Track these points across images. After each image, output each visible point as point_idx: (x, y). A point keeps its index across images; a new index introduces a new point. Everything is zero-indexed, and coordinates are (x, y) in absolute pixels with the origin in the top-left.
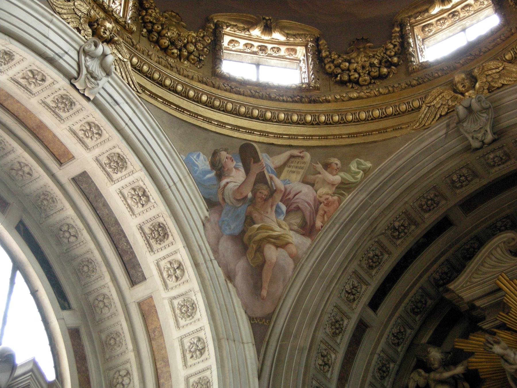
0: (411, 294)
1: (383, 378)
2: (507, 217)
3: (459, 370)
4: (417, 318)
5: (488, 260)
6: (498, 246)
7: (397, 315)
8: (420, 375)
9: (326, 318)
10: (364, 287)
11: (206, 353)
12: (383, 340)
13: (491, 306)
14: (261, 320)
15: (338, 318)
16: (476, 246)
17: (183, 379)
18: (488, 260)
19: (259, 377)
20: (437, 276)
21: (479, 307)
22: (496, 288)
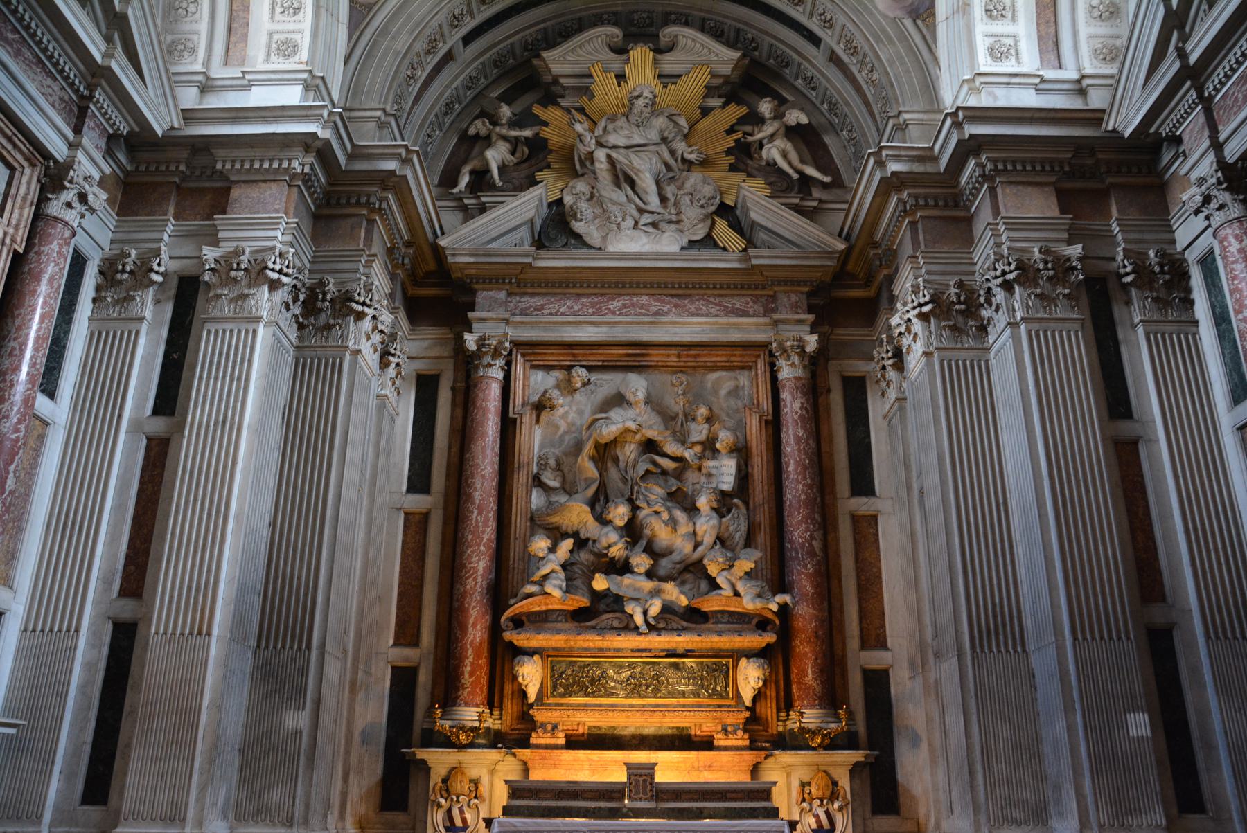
0: (502, 46)
1: (446, 114)
2: (615, 14)
3: (528, 133)
4: (495, 71)
5: (587, 44)
6: (600, 36)
7: (481, 60)
8: (484, 124)
9: (428, 32)
10: (469, 18)
11: (301, 15)
12: (461, 78)
13: (573, 88)
14: (360, 6)
15: (437, 37)
16: (575, 27)
17: (266, 33)
18: (587, 44)
19: (346, 63)
20: (530, 40)
21: (561, 85)
22: (587, 73)
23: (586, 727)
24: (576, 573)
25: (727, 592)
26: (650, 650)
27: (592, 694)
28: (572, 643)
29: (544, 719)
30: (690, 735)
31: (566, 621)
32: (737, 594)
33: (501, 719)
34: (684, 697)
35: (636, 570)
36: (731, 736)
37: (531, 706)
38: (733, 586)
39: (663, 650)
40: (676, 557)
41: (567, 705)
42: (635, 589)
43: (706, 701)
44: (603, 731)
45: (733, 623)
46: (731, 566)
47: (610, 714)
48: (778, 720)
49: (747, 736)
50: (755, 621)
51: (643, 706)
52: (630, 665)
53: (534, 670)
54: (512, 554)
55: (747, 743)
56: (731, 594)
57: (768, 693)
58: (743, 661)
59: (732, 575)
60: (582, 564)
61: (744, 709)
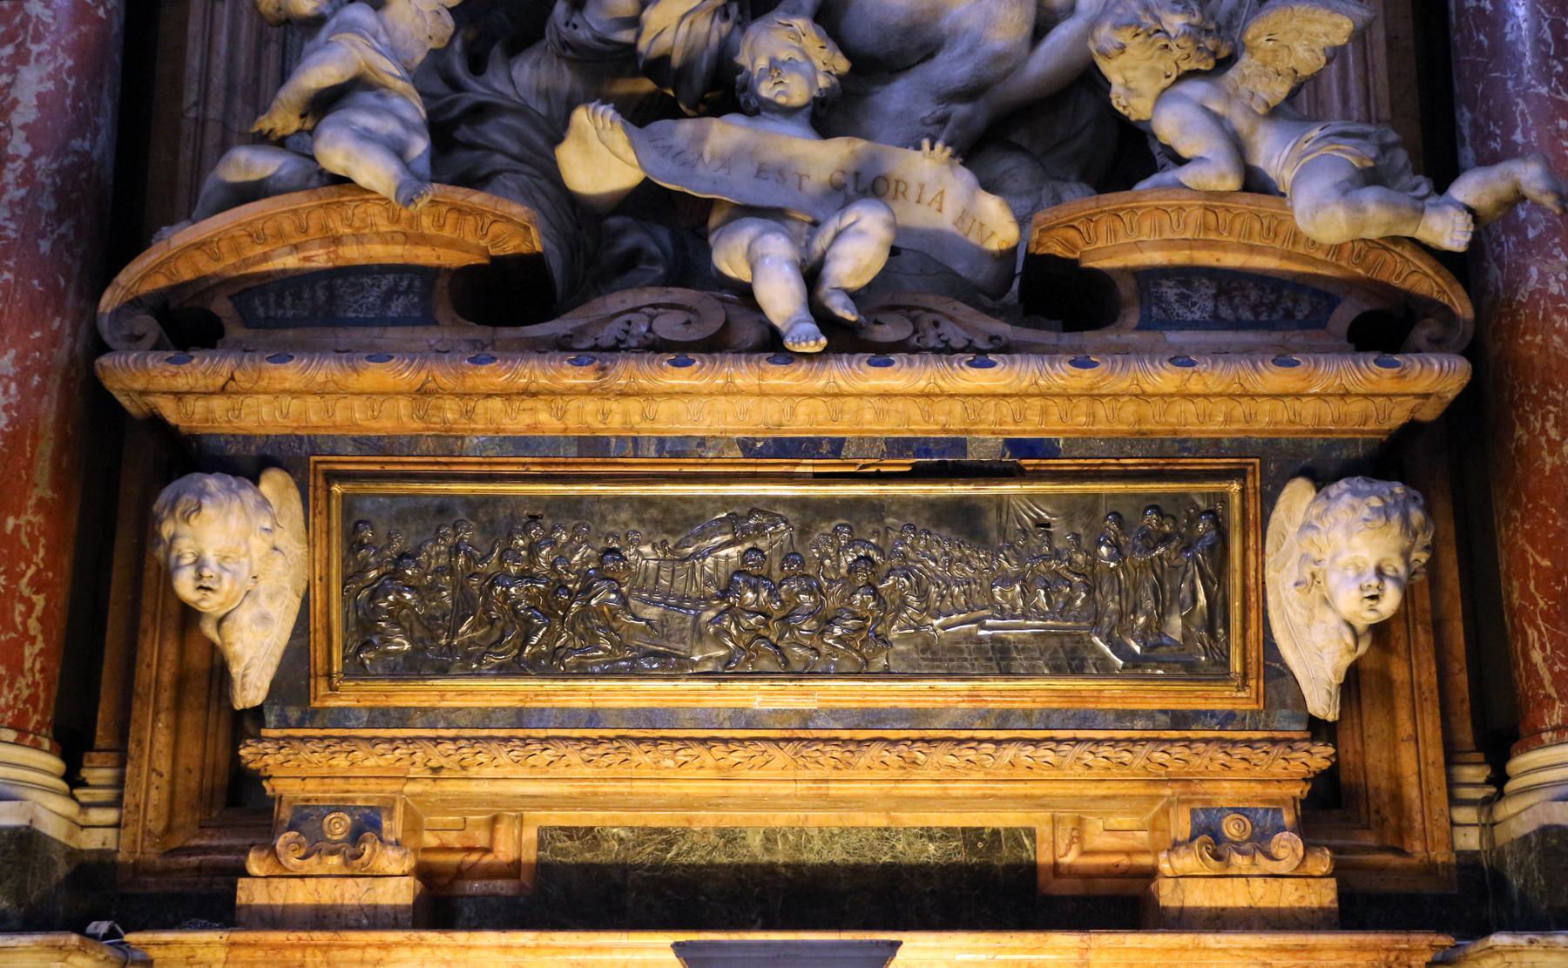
23: (531, 834)
24: (492, 149)
25: (1218, 175)
26: (837, 446)
27: (547, 666)
28: (450, 411)
29: (312, 789)
30: (1032, 868)
31: (428, 320)
32: (1254, 182)
33: (117, 803)
34: (1006, 673)
35: (766, 90)
36: (1240, 862)
37: (248, 723)
38: (1239, 147)
39: (898, 446)
40: (951, 69)
41: (430, 717)
42: (761, 172)
43: (1114, 693)
44: (609, 853)
45: (1238, 325)
46: (1224, 64)
47: (639, 755)
48: (1454, 801)
49: (1322, 863)
50: (1345, 314)
51: (806, 719)
52: (740, 518)
53: (258, 544)
54: (194, 61)
55: (1323, 895)
56: (1232, 183)
57: (1399, 671)
58: (1297, 497)
59: (1229, 98)
60: (521, 111)
61: (1298, 731)
